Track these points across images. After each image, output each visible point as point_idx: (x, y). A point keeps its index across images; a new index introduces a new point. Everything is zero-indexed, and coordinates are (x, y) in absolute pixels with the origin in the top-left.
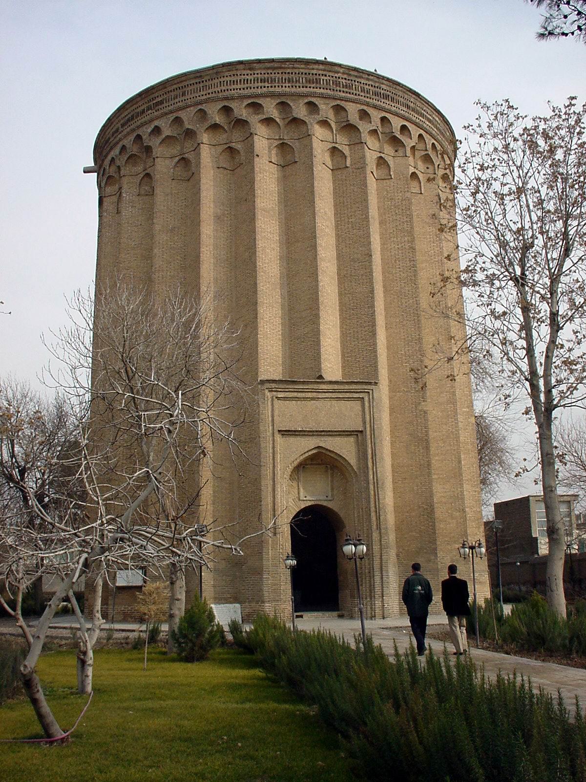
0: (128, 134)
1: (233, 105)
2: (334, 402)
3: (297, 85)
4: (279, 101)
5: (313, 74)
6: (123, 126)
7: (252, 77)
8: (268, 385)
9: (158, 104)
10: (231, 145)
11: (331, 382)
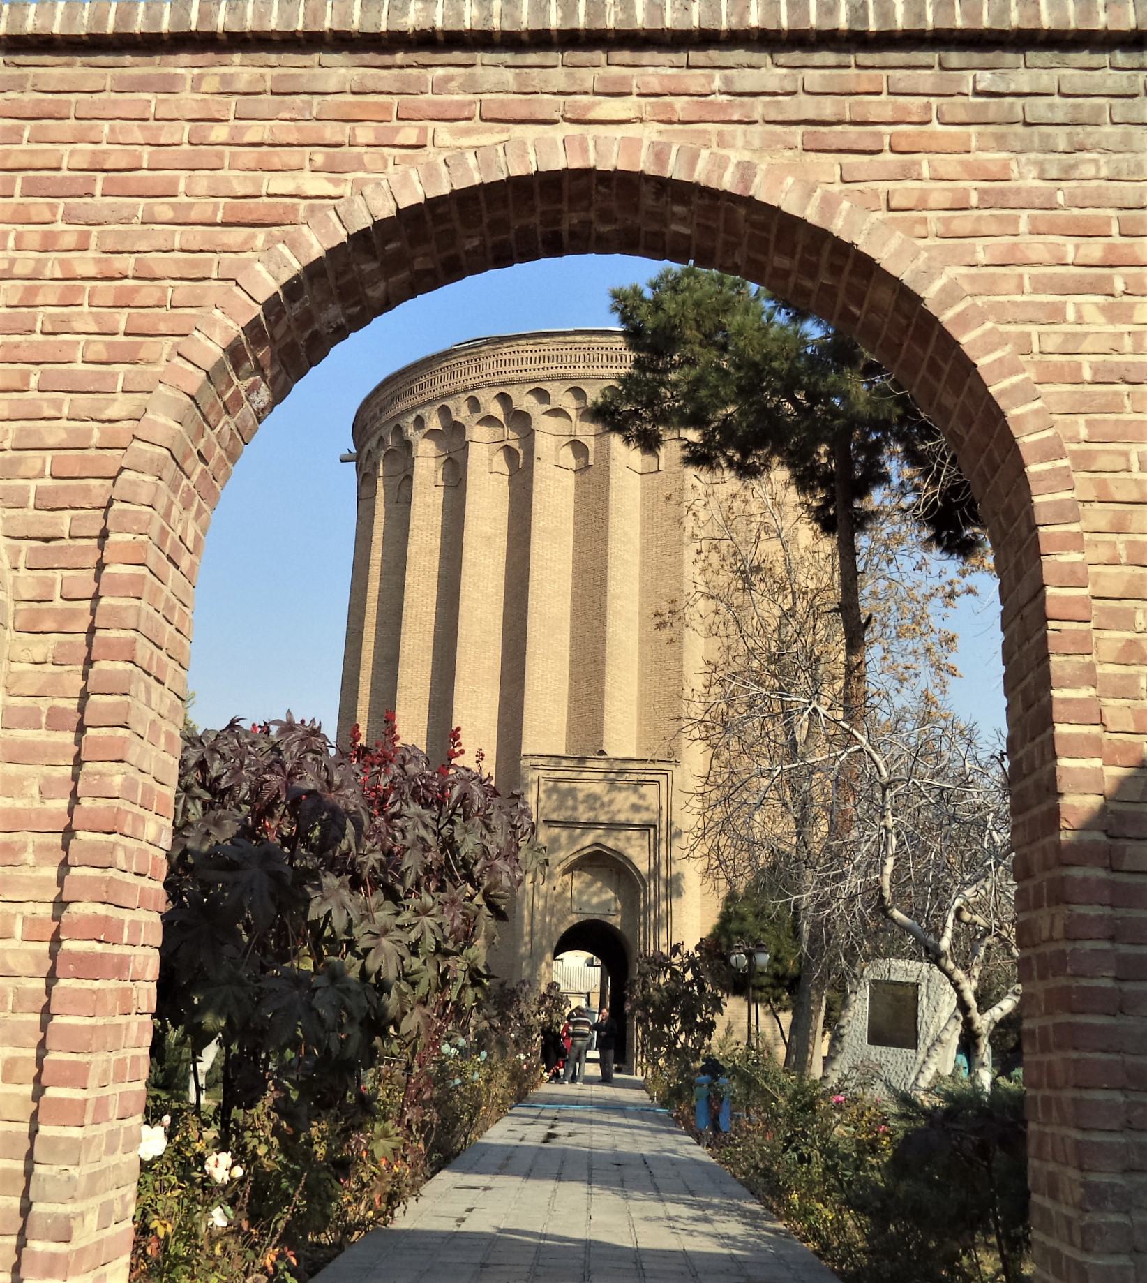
1: (511, 391)
3: (595, 364)
4: (571, 386)
7: (537, 355)
8: (534, 761)
10: (507, 443)
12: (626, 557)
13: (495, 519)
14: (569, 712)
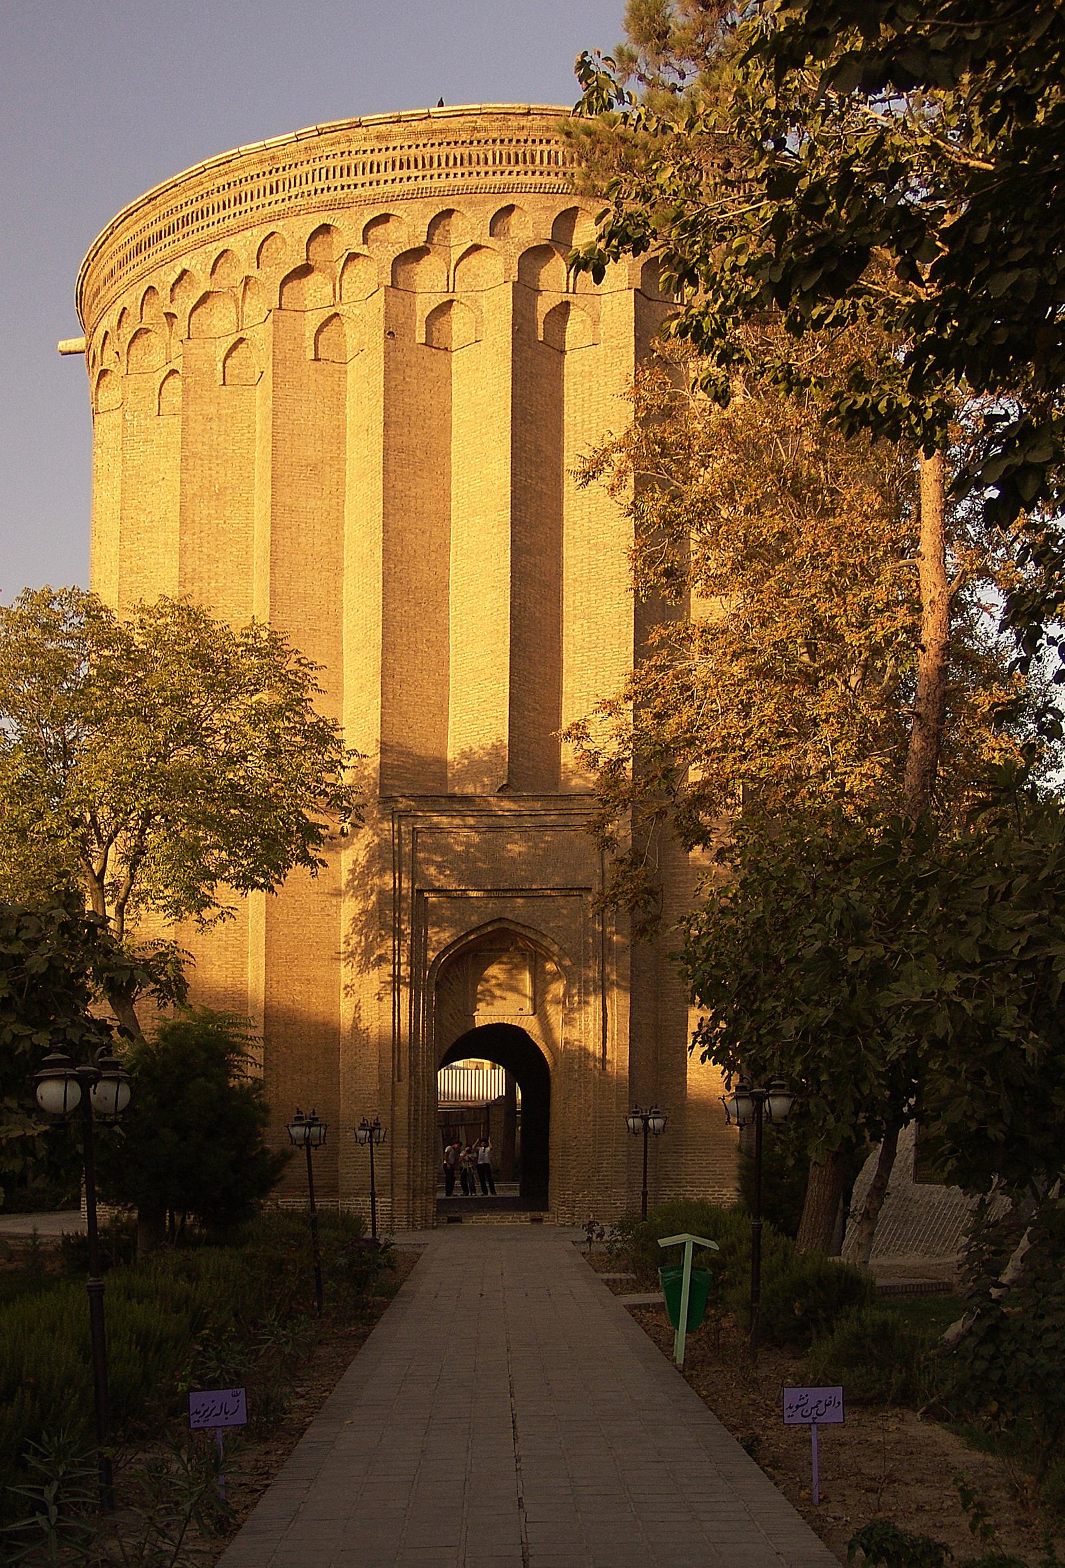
0: (132, 283)
5: (518, 141)
6: (121, 265)
7: (381, 157)
9: (185, 221)
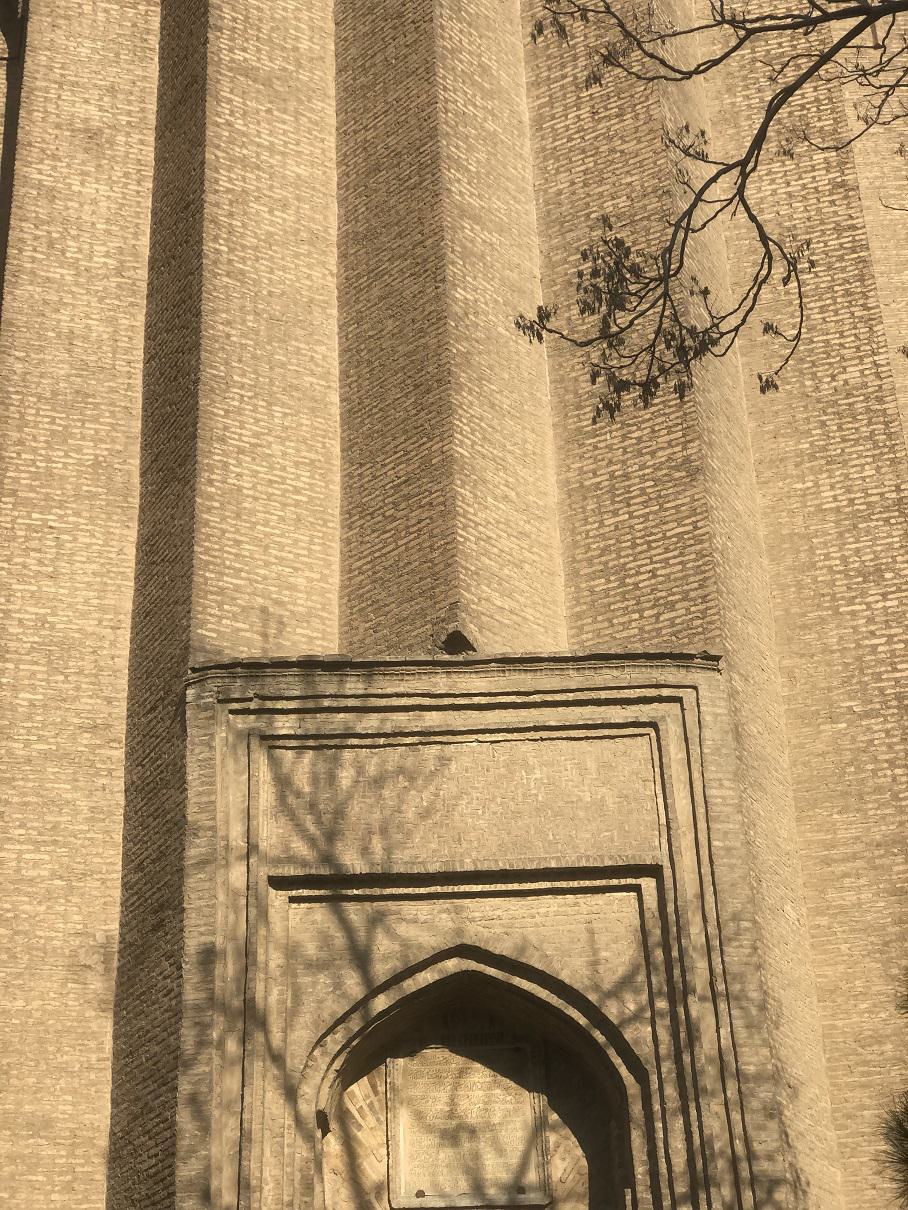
2: (526, 749)
11: (507, 662)
12: (490, 126)
13: (112, 90)
14: (347, 556)
